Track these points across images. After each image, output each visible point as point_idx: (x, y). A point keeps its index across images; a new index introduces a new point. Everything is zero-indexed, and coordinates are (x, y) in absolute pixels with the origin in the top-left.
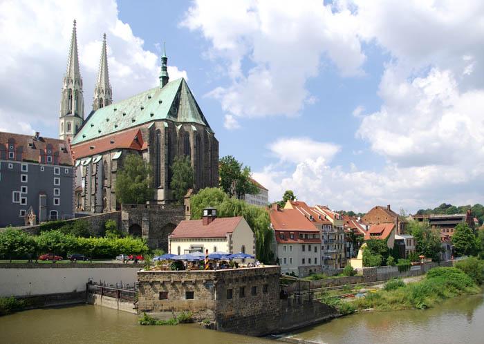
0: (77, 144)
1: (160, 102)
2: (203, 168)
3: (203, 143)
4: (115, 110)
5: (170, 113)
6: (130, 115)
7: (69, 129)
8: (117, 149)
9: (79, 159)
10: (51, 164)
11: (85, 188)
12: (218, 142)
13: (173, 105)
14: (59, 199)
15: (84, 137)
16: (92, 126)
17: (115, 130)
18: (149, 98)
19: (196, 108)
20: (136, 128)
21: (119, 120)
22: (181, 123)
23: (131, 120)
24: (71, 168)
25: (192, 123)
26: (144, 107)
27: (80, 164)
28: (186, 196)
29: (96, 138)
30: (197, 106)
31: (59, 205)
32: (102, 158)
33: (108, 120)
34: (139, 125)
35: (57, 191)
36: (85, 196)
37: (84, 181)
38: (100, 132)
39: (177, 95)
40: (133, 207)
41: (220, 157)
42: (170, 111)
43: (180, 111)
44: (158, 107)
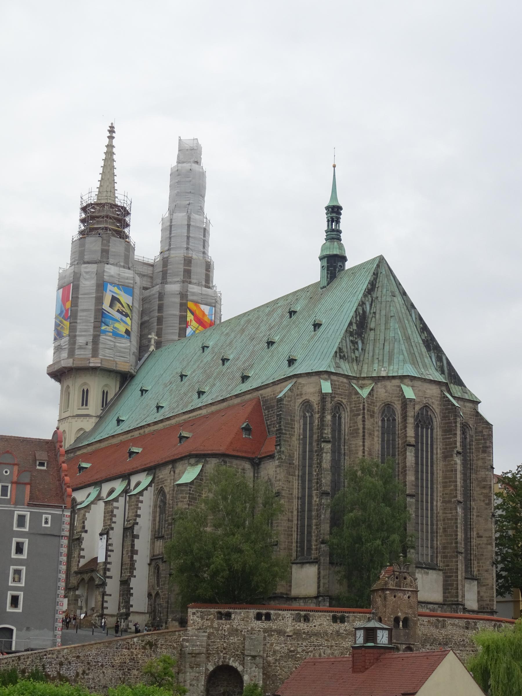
0: (100, 441)
1: (317, 326)
2: (439, 504)
3: (438, 432)
4: (204, 348)
5: (340, 354)
6: (239, 363)
7: (85, 401)
8: (190, 456)
9: (98, 483)
10: (9, 502)
11: (106, 563)
12: (489, 426)
13: (349, 332)
14: (21, 594)
15: (119, 421)
16: (143, 391)
17: (197, 403)
18: (292, 313)
19: (417, 338)
20: (248, 397)
21: (209, 377)
22: (372, 378)
23: (238, 375)
24: (58, 512)
25: (402, 378)
26: (276, 339)
27: (98, 498)
28: (375, 587)
29: (149, 425)
30: (424, 328)
31: (20, 610)
32: (152, 482)
33: (182, 376)
34: (257, 389)
35: (18, 572)
36: (103, 584)
37: (102, 544)
38: (158, 408)
39: (362, 304)
40: (220, 616)
41: (498, 471)
42: (340, 349)
43: (370, 347)
44: (312, 338)
